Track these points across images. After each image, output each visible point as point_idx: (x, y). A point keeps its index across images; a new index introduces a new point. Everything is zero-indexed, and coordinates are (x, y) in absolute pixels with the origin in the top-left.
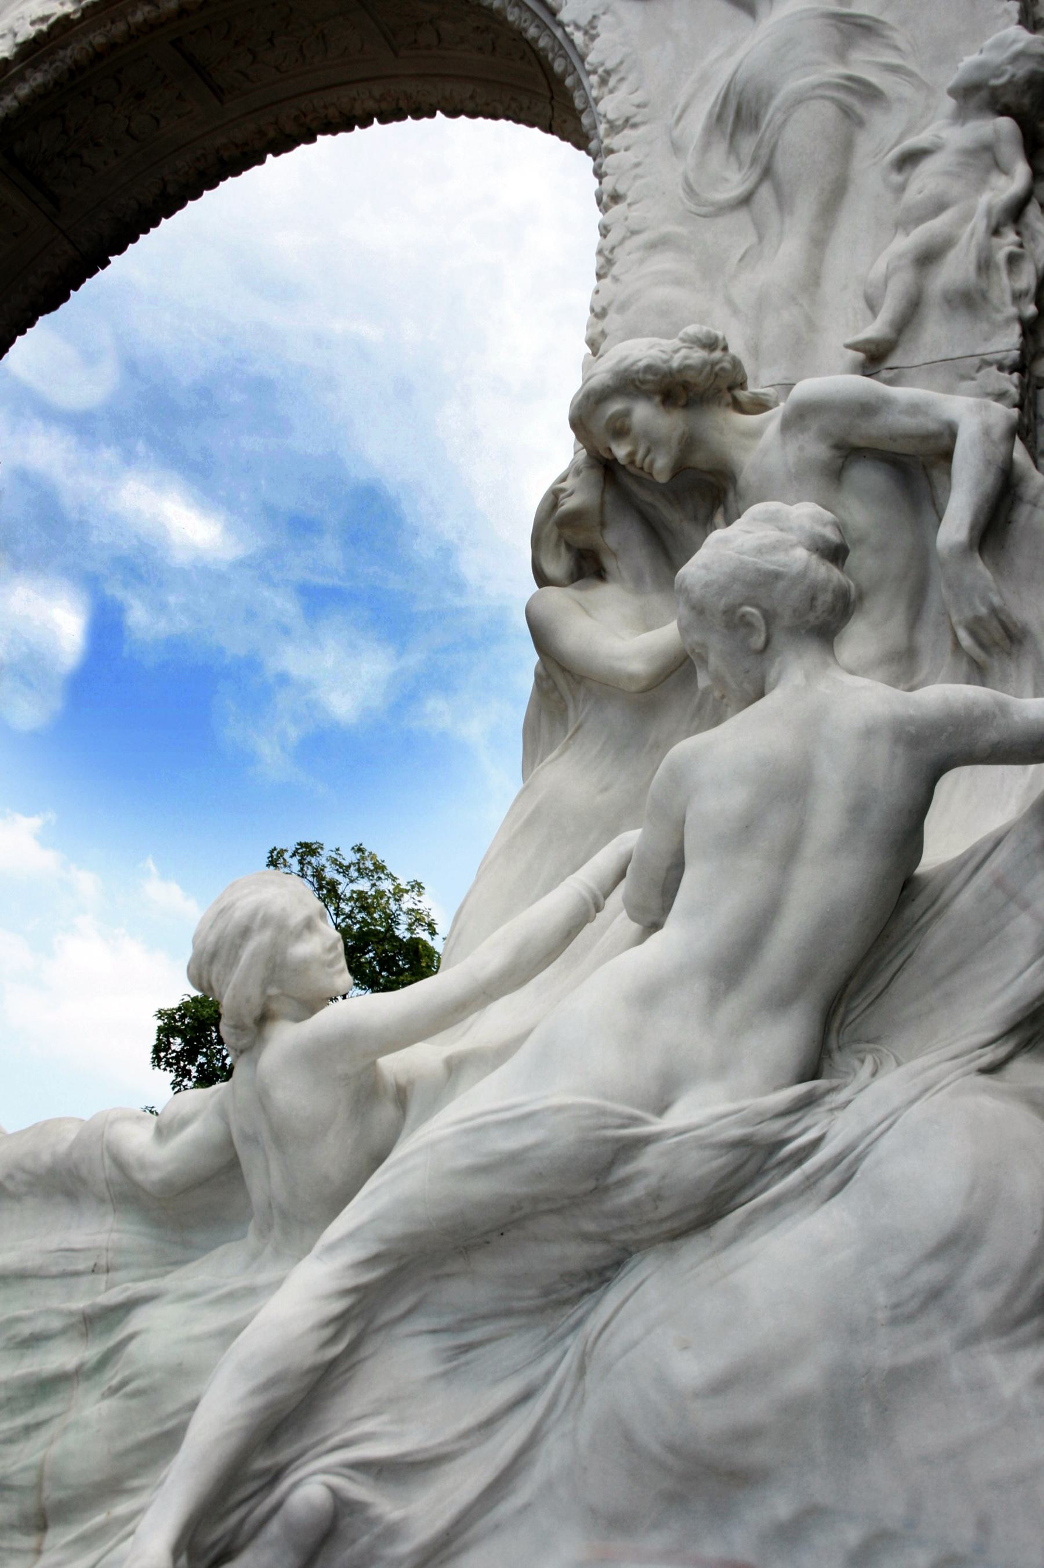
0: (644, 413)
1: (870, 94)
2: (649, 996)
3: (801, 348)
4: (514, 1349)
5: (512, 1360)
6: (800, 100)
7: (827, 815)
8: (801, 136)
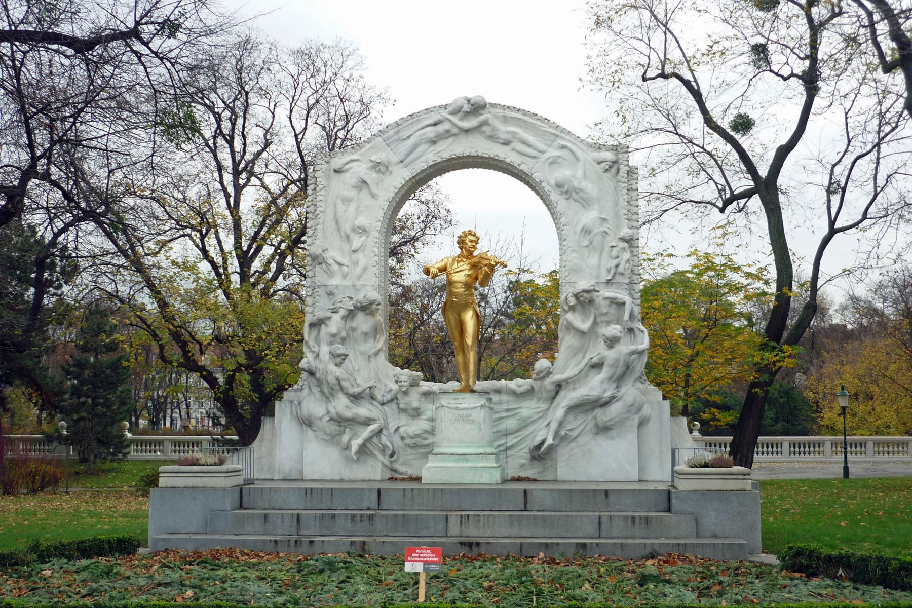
0: (585, 295)
1: (606, 233)
2: (602, 382)
3: (598, 276)
4: (581, 416)
5: (581, 418)
6: (597, 234)
7: (621, 363)
8: (597, 240)
